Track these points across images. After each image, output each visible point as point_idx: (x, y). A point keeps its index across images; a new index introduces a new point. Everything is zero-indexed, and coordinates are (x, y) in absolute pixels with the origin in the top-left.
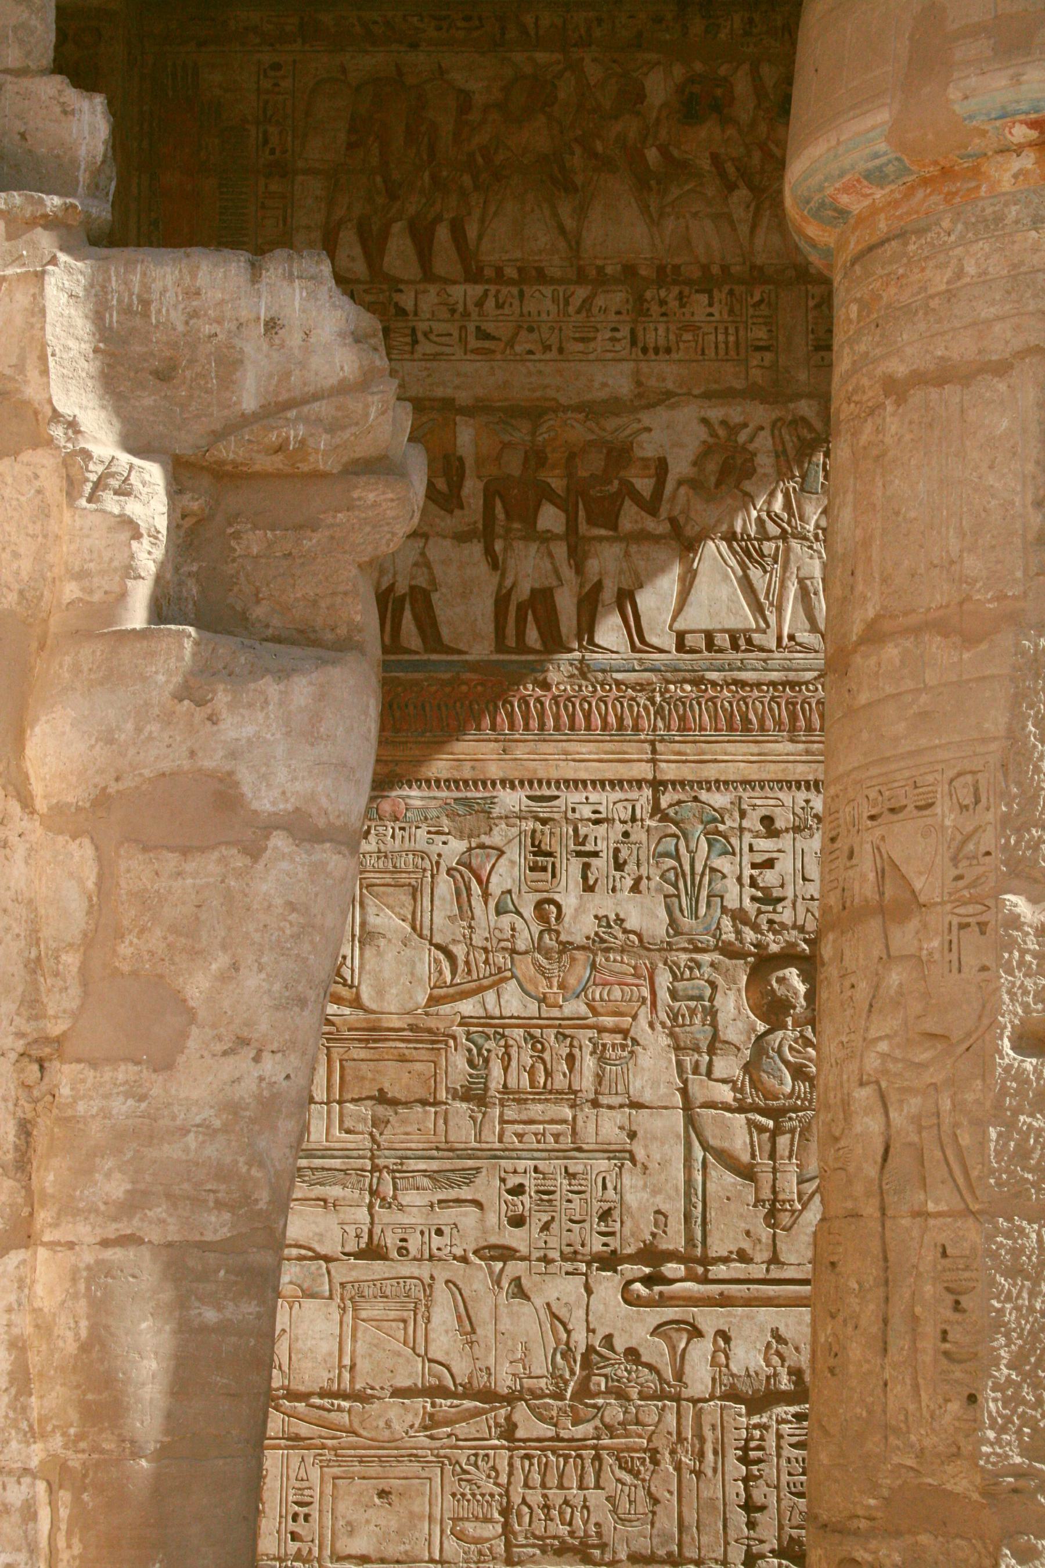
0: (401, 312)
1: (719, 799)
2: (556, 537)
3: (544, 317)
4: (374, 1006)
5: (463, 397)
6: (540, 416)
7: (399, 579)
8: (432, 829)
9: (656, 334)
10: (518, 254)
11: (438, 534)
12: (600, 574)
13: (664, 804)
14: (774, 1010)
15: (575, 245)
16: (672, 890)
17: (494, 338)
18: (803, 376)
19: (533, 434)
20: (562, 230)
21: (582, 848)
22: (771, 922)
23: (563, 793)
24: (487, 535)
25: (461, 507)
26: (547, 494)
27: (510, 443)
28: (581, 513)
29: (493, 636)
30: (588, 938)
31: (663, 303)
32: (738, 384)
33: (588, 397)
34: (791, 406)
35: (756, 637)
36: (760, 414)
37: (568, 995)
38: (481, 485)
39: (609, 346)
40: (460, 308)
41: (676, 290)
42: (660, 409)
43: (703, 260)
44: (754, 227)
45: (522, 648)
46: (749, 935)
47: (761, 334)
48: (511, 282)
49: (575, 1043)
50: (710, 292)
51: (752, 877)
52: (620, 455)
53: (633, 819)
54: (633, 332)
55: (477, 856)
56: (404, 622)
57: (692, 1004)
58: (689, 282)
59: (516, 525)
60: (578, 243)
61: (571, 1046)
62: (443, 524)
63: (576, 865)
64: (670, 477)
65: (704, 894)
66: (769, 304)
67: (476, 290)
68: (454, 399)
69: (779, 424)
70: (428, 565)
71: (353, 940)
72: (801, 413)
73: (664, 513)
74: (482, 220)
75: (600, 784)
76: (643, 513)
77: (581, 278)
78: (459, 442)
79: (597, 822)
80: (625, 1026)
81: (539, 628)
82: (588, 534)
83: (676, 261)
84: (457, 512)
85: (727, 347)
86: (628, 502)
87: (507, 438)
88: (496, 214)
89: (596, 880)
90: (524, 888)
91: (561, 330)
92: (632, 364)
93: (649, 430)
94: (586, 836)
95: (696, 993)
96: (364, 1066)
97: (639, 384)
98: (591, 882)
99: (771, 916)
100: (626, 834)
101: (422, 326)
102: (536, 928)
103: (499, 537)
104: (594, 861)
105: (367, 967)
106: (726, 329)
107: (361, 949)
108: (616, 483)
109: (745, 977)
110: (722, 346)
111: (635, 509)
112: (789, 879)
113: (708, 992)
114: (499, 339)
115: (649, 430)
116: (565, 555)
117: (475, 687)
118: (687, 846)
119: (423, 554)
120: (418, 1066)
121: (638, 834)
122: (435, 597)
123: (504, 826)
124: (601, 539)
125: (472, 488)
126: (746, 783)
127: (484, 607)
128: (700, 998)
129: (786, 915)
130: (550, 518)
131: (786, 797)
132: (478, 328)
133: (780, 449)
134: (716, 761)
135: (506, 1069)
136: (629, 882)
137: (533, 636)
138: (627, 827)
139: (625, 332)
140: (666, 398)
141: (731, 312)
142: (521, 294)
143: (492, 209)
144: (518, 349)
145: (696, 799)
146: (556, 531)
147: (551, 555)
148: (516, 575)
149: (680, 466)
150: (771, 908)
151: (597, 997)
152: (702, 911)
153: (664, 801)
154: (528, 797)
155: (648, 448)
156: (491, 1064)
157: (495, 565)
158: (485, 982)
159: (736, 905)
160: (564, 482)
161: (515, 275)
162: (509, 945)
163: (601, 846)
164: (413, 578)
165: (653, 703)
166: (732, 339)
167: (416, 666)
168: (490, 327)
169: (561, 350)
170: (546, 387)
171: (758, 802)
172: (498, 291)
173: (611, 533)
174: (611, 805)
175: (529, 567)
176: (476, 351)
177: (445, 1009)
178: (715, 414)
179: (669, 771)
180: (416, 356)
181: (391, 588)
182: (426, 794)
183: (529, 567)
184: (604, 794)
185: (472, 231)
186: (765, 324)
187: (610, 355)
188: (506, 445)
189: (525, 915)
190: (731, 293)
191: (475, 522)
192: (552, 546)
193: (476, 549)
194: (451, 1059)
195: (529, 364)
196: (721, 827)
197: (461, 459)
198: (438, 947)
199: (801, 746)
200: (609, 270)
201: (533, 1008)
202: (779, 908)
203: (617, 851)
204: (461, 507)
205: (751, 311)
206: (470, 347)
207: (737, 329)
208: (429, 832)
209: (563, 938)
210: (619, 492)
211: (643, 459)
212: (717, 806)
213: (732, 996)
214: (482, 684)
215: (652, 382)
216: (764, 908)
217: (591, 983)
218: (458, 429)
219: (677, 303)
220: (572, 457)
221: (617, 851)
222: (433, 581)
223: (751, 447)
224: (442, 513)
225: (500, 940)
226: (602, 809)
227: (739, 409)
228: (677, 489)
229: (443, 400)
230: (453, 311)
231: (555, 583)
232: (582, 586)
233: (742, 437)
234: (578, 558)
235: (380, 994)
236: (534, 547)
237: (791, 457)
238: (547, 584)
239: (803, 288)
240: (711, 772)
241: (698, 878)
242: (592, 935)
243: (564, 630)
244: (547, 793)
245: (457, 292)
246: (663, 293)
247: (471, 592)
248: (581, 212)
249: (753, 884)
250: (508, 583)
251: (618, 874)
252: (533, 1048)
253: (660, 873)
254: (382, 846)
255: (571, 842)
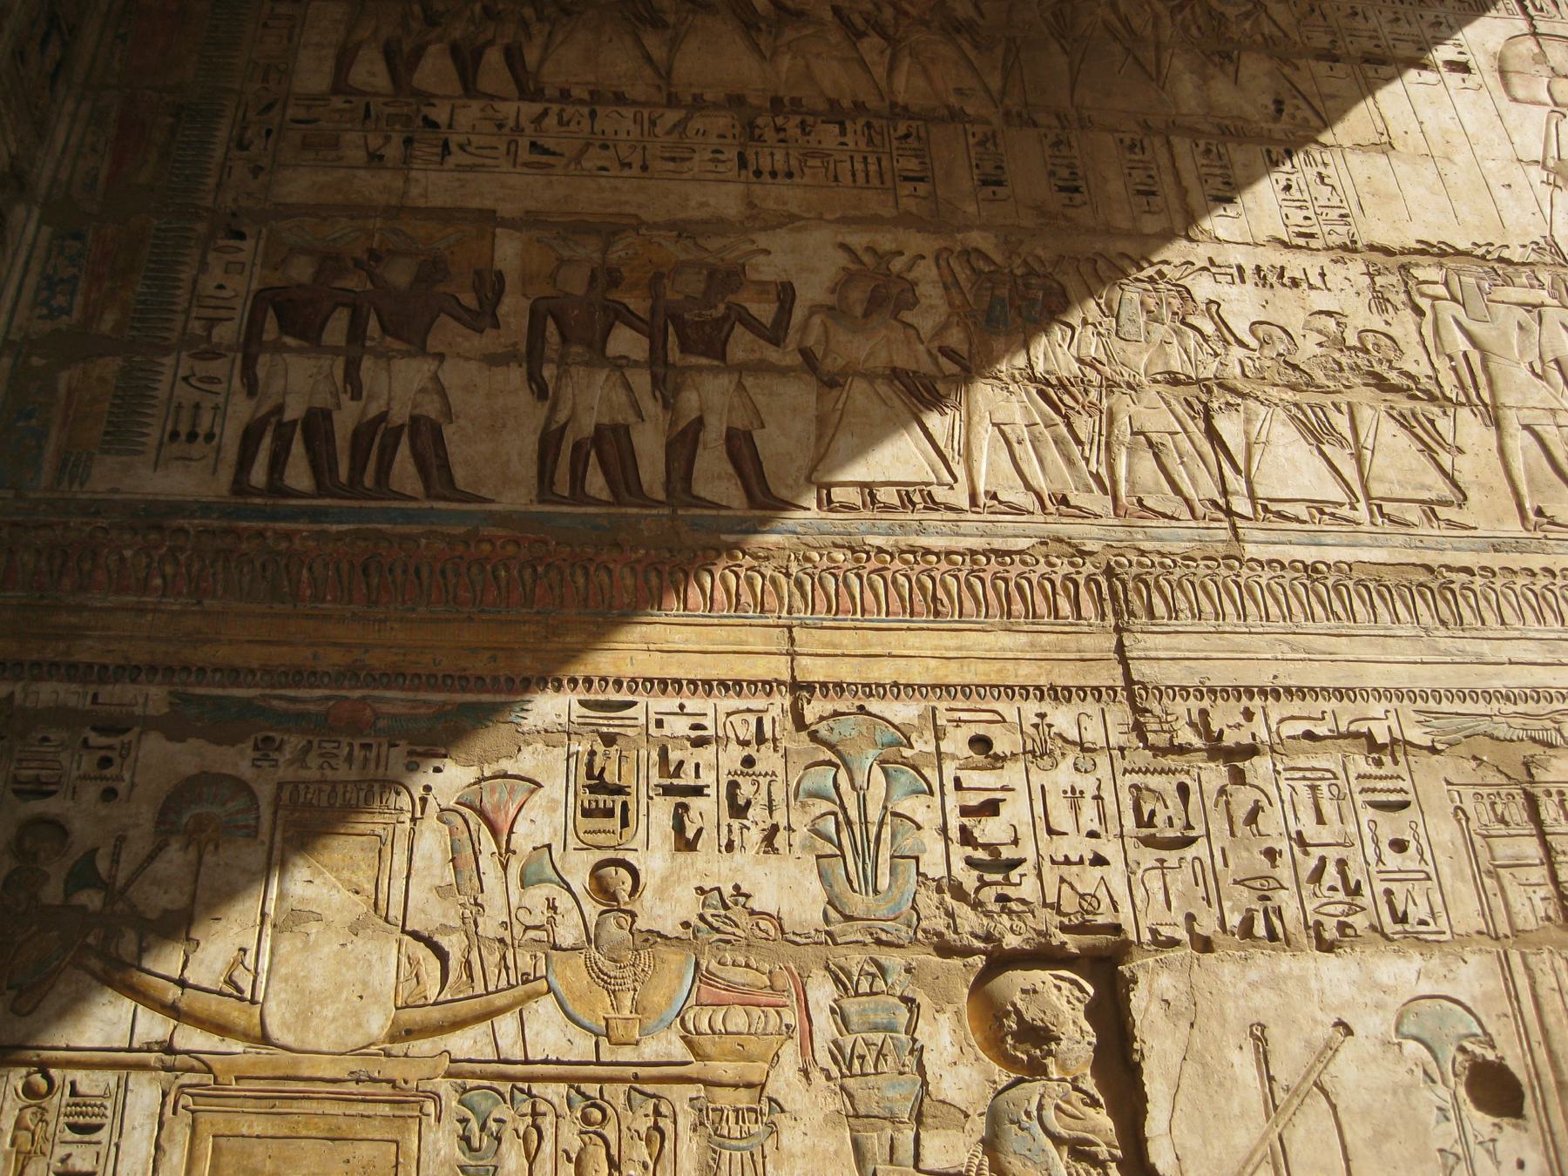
0: (431, 124)
1: (903, 711)
2: (636, 364)
3: (623, 136)
4: (288, 1039)
5: (507, 209)
6: (614, 234)
7: (396, 407)
8: (419, 749)
9: (772, 156)
10: (591, 78)
11: (458, 355)
12: (701, 410)
13: (809, 717)
14: (1020, 1044)
15: (665, 74)
16: (829, 849)
17: (554, 154)
18: (971, 209)
19: (604, 252)
20: (649, 59)
21: (676, 781)
22: (1002, 899)
23: (641, 699)
24: (533, 358)
25: (497, 326)
26: (622, 315)
27: (570, 261)
28: (672, 339)
29: (535, 481)
30: (686, 925)
31: (779, 130)
32: (888, 212)
33: (681, 215)
34: (959, 236)
35: (940, 494)
36: (917, 242)
37: (649, 1023)
38: (526, 304)
39: (711, 166)
40: (511, 123)
41: (798, 119)
42: (782, 232)
43: (832, 95)
44: (891, 69)
45: (578, 494)
46: (969, 920)
47: (912, 165)
48: (581, 102)
49: (664, 1109)
50: (842, 124)
51: (963, 829)
52: (728, 278)
53: (761, 739)
54: (741, 156)
55: (493, 790)
56: (398, 457)
57: (877, 1038)
58: (814, 113)
59: (576, 349)
60: (669, 73)
61: (657, 1112)
62: (467, 345)
63: (663, 810)
64: (797, 302)
65: (885, 854)
66: (919, 138)
67: (531, 109)
68: (494, 212)
69: (945, 255)
70: (443, 393)
71: (262, 923)
72: (974, 244)
73: (792, 339)
74: (546, 47)
75: (707, 686)
76: (762, 342)
77: (672, 101)
78: (498, 254)
79: (699, 743)
80: (756, 1079)
81: (606, 473)
82: (680, 364)
83: (795, 94)
84: (490, 332)
85: (867, 175)
86: (739, 329)
87: (566, 253)
88: (562, 43)
89: (699, 832)
90: (573, 842)
91: (644, 148)
92: (742, 187)
93: (768, 252)
94: (681, 763)
95: (882, 1018)
96: (259, 1149)
97: (751, 205)
98: (690, 834)
99: (999, 889)
100: (748, 762)
101: (454, 139)
102: (592, 909)
103: (552, 361)
104: (695, 803)
105: (283, 971)
106: (865, 158)
107: (273, 940)
108: (722, 307)
109: (966, 991)
110: (861, 177)
111: (749, 336)
112: (1025, 832)
113: (903, 1016)
114: (562, 155)
115: (768, 252)
116: (649, 387)
117: (503, 547)
118: (852, 780)
119: (435, 378)
120: (364, 1151)
121: (767, 760)
122: (448, 431)
123: (540, 746)
124: (700, 369)
125: (515, 309)
126: (945, 689)
127: (522, 447)
128: (890, 1028)
129: (1028, 889)
130: (625, 342)
131: (1007, 709)
132: (533, 144)
133: (950, 280)
134: (890, 656)
135: (531, 1159)
136: (755, 836)
137: (596, 483)
138: (751, 751)
139: (731, 154)
140: (788, 220)
141: (870, 141)
142: (593, 114)
143: (559, 38)
144: (585, 164)
145: (861, 708)
146: (634, 357)
147: (628, 387)
148: (574, 409)
149: (811, 291)
150: (999, 877)
151: (704, 1027)
152: (884, 882)
153: (811, 712)
154: (583, 703)
155: (767, 269)
156: (504, 1146)
157: (542, 393)
158: (500, 1000)
159: (940, 871)
160: (649, 303)
161: (586, 96)
162: (542, 935)
163: (707, 778)
164: (415, 406)
165: (788, 575)
166: (873, 168)
167: (408, 517)
168: (549, 143)
169: (644, 168)
170: (626, 203)
171: (964, 716)
172: (562, 110)
173: (716, 363)
174: (722, 718)
175: (592, 399)
176: (525, 164)
177: (422, 1046)
178: (858, 240)
179: (814, 670)
180: (446, 166)
181: (383, 417)
182: (411, 695)
183: (592, 399)
184: (711, 701)
185: (532, 56)
186: (916, 156)
187: (712, 176)
188: (562, 262)
189: (577, 887)
190: (869, 125)
191: (515, 344)
192: (628, 373)
193: (516, 375)
194: (428, 1137)
195: (603, 181)
196: (907, 752)
197: (500, 276)
198: (416, 936)
199: (1023, 638)
200: (709, 96)
201: (583, 1047)
202: (1014, 876)
203: (733, 786)
204: (497, 326)
205: (895, 143)
206: (519, 160)
207: (879, 160)
208: (411, 753)
209: (641, 924)
210: (725, 318)
211: (763, 283)
212: (896, 721)
213: (946, 1021)
214: (517, 543)
215: (770, 204)
216: (988, 877)
217: (692, 1000)
218: (497, 241)
219: (799, 131)
220: (659, 276)
221: (733, 786)
222: (448, 414)
223: (911, 276)
224: (467, 331)
225: (527, 928)
226: (708, 722)
227: (889, 236)
228: (810, 316)
229: (480, 210)
230: (500, 126)
231: (632, 419)
232: (673, 424)
233: (897, 265)
234: (666, 384)
235: (304, 1017)
236: (601, 376)
237: (966, 290)
238: (620, 419)
239: (960, 126)
240: (883, 672)
241: (873, 830)
242: (694, 920)
243: (645, 477)
244: (613, 696)
245: (508, 109)
246: (780, 121)
247: (504, 426)
248: (674, 45)
249: (967, 838)
250: (562, 416)
251: (736, 824)
252: (586, 1119)
253: (808, 819)
254: (329, 773)
255: (654, 772)
